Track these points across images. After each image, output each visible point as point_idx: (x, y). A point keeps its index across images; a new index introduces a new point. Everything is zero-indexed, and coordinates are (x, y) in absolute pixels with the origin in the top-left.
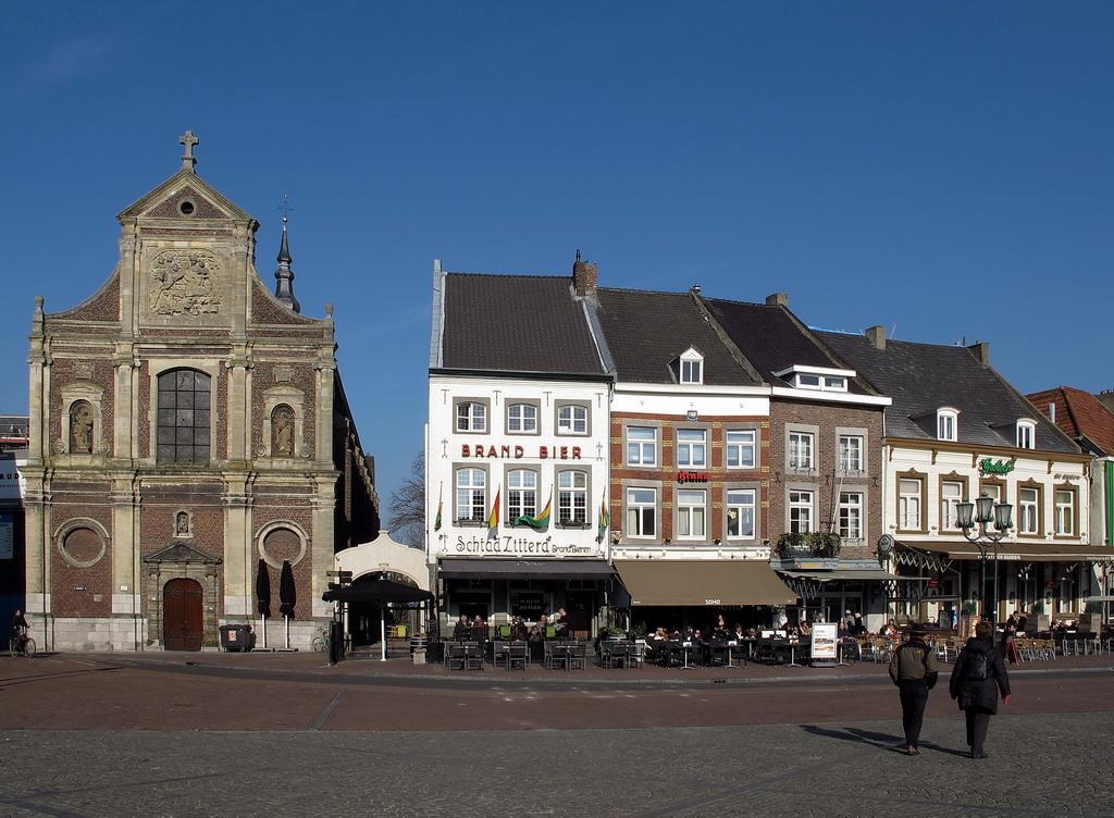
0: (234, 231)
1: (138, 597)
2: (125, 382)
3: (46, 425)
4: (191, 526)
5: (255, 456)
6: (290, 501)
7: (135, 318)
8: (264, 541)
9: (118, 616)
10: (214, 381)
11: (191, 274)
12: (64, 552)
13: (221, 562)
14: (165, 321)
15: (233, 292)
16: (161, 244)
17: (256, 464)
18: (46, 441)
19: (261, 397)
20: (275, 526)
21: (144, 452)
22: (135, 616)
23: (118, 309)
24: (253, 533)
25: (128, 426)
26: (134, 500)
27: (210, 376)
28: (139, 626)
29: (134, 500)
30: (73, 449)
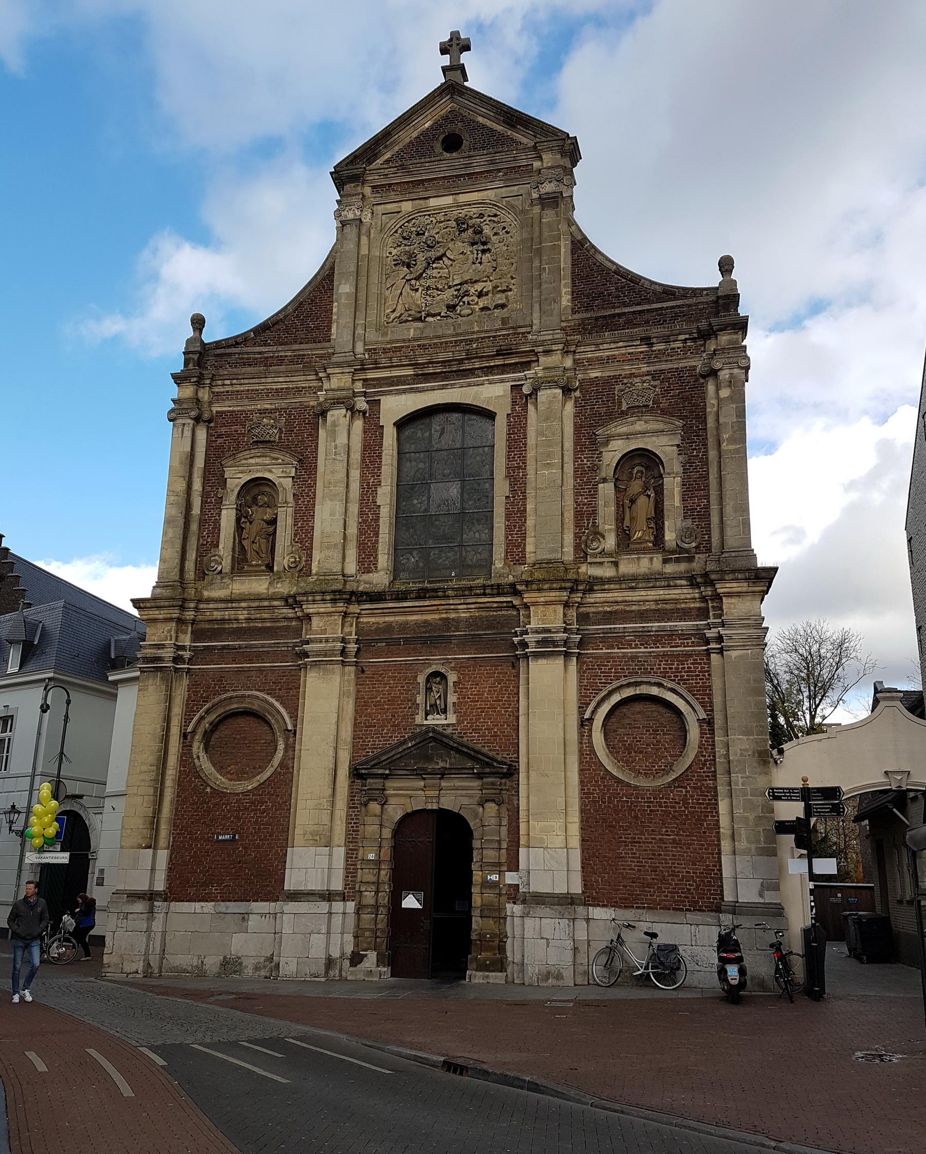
0: (537, 164)
1: (340, 853)
2: (339, 437)
3: (194, 527)
4: (452, 698)
6: (659, 638)
7: (360, 331)
8: (604, 725)
9: (295, 896)
10: (501, 422)
11: (459, 247)
12: (205, 763)
13: (512, 772)
15: (536, 263)
16: (407, 207)
17: (585, 570)
18: (192, 555)
20: (628, 692)
21: (367, 561)
22: (328, 896)
23: (330, 322)
24: (582, 709)
25: (339, 517)
26: (343, 652)
27: (490, 416)
28: (337, 920)
29: (343, 652)
30: (240, 565)
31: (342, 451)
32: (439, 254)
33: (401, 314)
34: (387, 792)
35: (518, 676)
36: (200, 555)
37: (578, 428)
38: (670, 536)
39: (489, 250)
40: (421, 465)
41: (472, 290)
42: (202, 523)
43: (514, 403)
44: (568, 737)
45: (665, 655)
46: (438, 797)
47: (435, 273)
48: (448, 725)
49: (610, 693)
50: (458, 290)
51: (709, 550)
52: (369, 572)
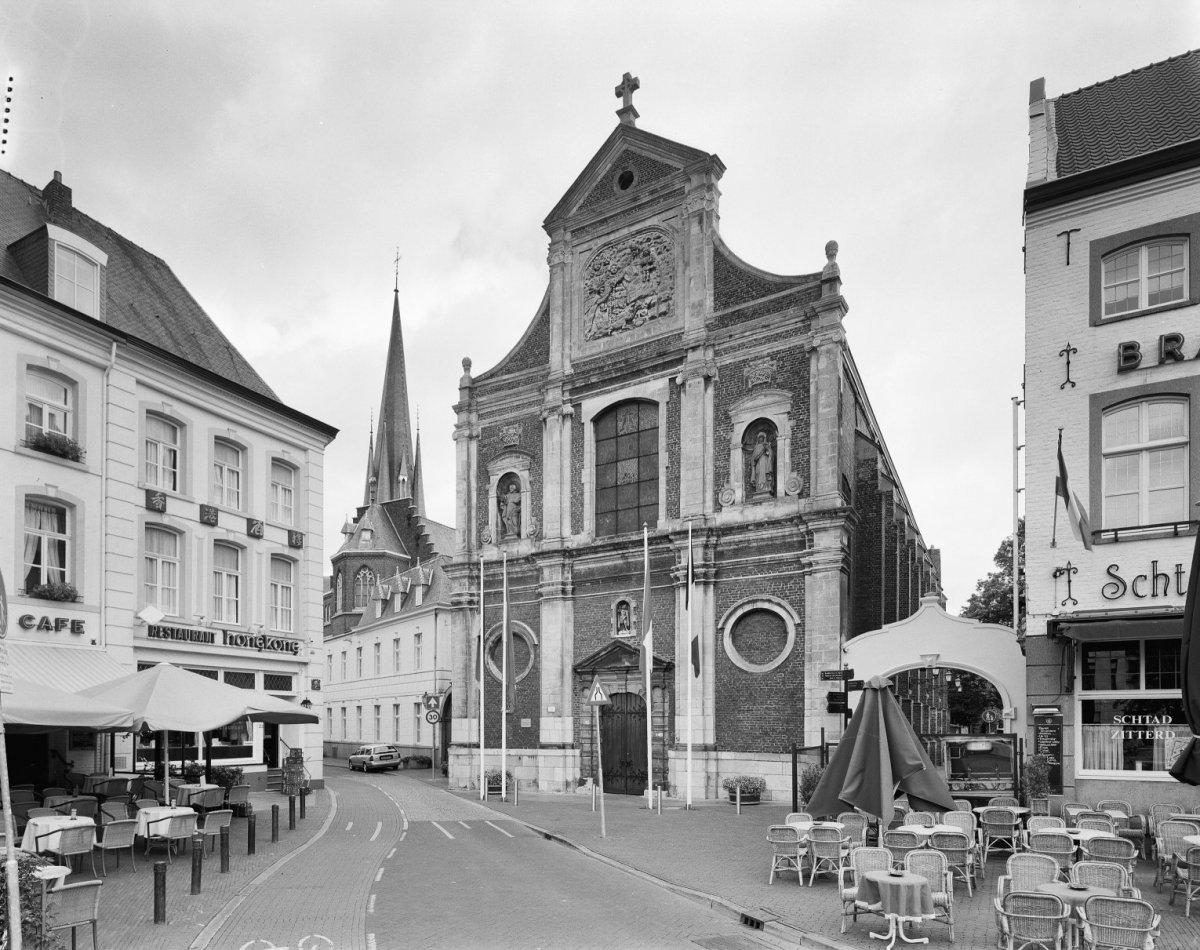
4: (634, 619)
5: (718, 507)
7: (567, 351)
10: (663, 410)
14: (601, 346)
20: (747, 608)
21: (577, 527)
24: (717, 622)
26: (564, 591)
27: (655, 404)
31: (557, 447)
35: (674, 601)
36: (479, 532)
37: (717, 407)
38: (781, 488)
39: (654, 269)
42: (479, 508)
43: (671, 393)
44: (706, 642)
45: (775, 578)
47: (617, 295)
48: (631, 637)
49: (736, 609)
50: (633, 306)
51: (808, 495)
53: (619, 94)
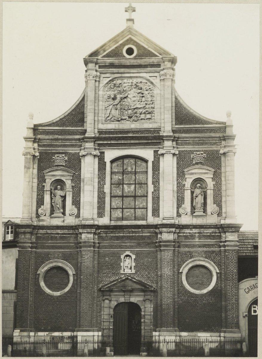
5: (179, 215)
10: (150, 165)
19: (184, 175)
21: (101, 214)
27: (146, 161)
32: (125, 96)
33: (111, 118)
34: (112, 296)
40: (120, 178)
41: (138, 112)
43: (155, 157)
46: (130, 298)
52: (102, 217)
53: (126, 11)
